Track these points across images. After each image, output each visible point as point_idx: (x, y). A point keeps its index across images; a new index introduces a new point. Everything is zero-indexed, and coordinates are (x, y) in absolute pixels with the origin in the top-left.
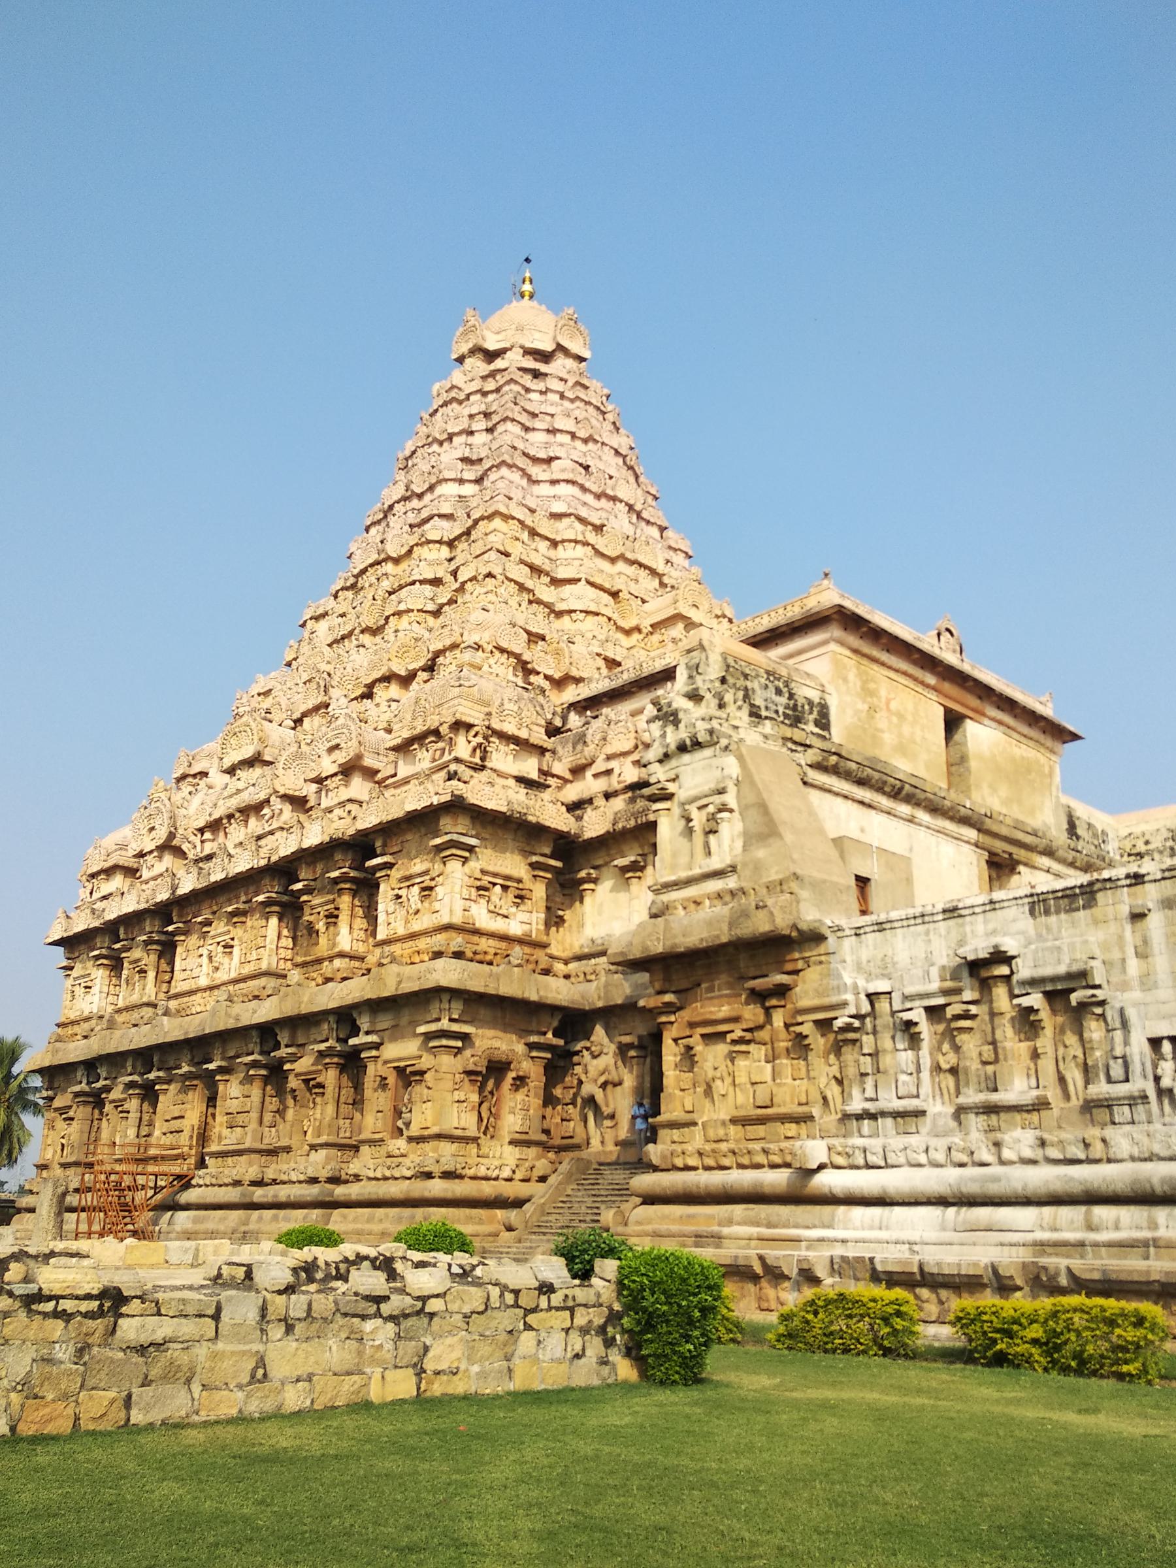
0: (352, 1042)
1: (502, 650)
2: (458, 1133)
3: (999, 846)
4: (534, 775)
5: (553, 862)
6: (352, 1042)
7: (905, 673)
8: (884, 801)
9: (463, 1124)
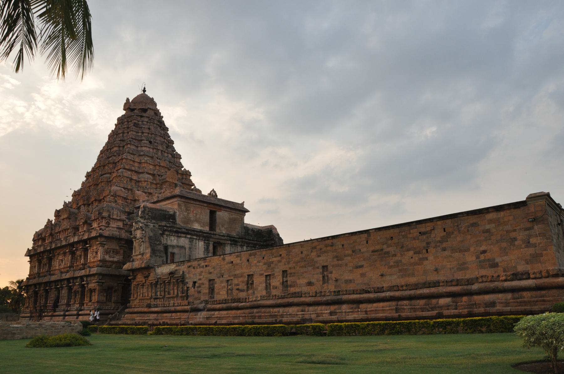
0: (83, 283)
1: (119, 196)
2: (101, 301)
3: (216, 241)
4: (122, 227)
5: (124, 245)
6: (83, 283)
7: (198, 204)
8: (184, 235)
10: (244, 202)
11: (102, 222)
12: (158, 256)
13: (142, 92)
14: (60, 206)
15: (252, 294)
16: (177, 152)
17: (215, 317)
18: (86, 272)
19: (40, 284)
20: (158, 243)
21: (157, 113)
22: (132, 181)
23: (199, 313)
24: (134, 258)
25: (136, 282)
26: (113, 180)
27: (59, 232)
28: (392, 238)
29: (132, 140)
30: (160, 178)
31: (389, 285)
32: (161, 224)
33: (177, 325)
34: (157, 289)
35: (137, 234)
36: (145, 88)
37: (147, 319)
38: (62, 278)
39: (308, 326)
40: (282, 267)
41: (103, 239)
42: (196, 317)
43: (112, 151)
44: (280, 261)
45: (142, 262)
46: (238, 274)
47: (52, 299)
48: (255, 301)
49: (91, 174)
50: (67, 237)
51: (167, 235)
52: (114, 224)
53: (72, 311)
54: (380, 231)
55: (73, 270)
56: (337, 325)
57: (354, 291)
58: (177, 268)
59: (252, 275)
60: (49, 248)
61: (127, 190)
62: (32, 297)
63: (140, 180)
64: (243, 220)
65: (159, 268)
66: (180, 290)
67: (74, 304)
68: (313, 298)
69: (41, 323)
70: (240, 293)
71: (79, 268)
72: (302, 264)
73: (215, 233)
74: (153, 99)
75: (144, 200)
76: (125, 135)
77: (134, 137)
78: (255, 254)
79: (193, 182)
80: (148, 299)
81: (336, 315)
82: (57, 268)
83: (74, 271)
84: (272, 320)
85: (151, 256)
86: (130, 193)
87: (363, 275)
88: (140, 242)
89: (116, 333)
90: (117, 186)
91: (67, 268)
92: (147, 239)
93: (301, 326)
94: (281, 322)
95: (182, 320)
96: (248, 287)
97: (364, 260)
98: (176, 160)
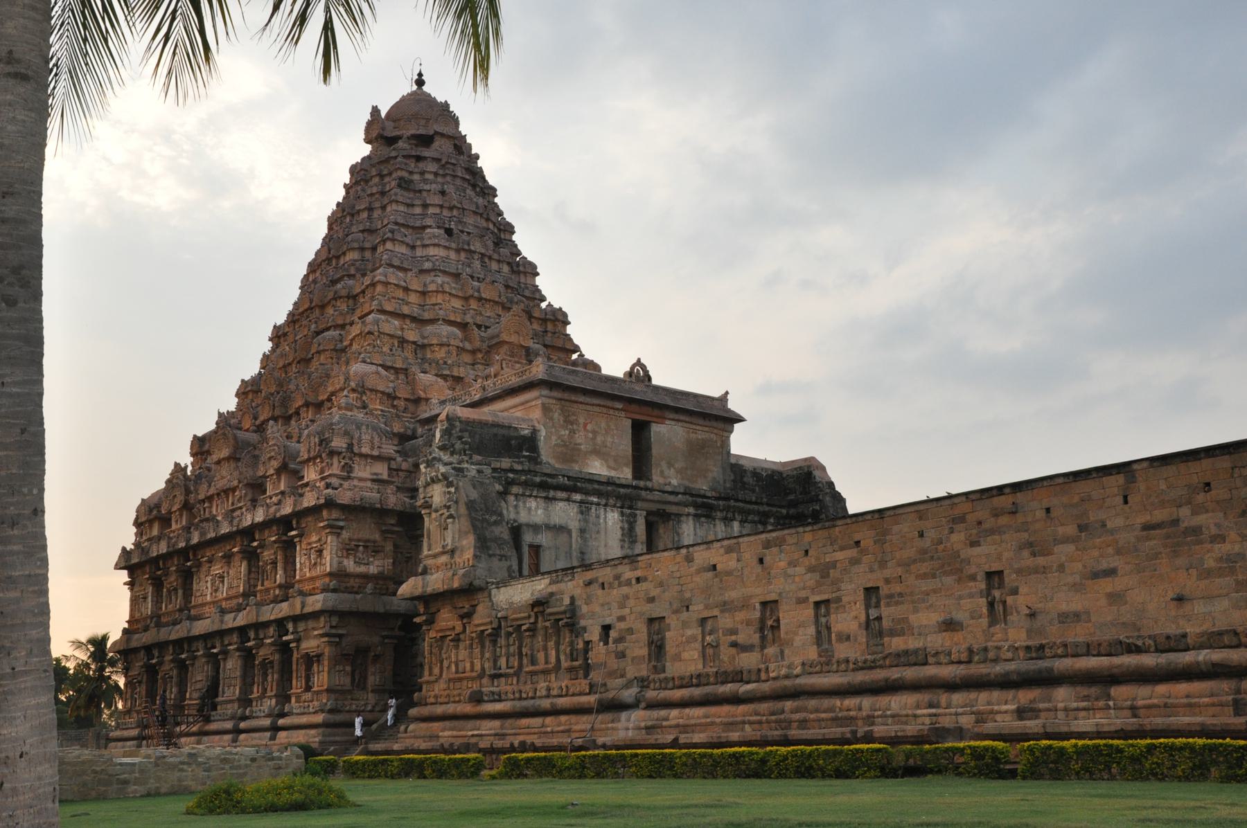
0: (284, 638)
1: (371, 390)
2: (339, 688)
3: (654, 507)
4: (385, 477)
5: (396, 529)
6: (284, 638)
7: (599, 405)
9: (342, 683)
10: (727, 393)
11: (332, 464)
12: (494, 555)
13: (415, 87)
14: (207, 425)
15: (777, 656)
16: (524, 258)
17: (670, 727)
18: (292, 606)
19: (162, 646)
20: (494, 518)
21: (460, 145)
22: (405, 345)
23: (624, 715)
24: (430, 562)
25: (438, 631)
26: (351, 345)
27: (210, 499)
28: (1208, 484)
29: (396, 227)
30: (483, 334)
31: (1204, 628)
32: (498, 465)
33: (560, 748)
34: (498, 650)
35: (432, 497)
36: (420, 75)
37: (473, 736)
38: (224, 627)
39: (957, 749)
40: (862, 577)
41: (335, 514)
42: (614, 725)
43: (342, 262)
44: (855, 562)
45: (453, 575)
46: (733, 601)
47: (199, 686)
48: (787, 677)
49: (287, 330)
50: (233, 511)
51: (516, 495)
52: (365, 470)
53: (257, 717)
54: (1166, 465)
55: (255, 604)
56: (1050, 747)
57: (1088, 645)
58: (554, 588)
59: (776, 601)
60: (182, 545)
61: (392, 371)
62: (140, 682)
63: (426, 341)
64: (725, 444)
65: (502, 589)
66: (565, 650)
67: (263, 696)
68: (962, 667)
69: (193, 751)
70: (743, 655)
71: (271, 596)
72: (924, 568)
73: (649, 484)
74: (446, 105)
75: (443, 398)
76: (376, 214)
77: (402, 222)
78: (780, 543)
79: (576, 342)
80: (473, 679)
81: (1037, 717)
82: (208, 598)
83: (259, 605)
84: (843, 733)
85: (475, 556)
86: (403, 380)
87: (1115, 598)
88: (444, 516)
89: (392, 777)
90: (364, 362)
91: (236, 597)
92: (463, 510)
93: (936, 748)
94: (868, 738)
95: (574, 735)
96: (763, 638)
97: (1119, 552)
98: (522, 280)
